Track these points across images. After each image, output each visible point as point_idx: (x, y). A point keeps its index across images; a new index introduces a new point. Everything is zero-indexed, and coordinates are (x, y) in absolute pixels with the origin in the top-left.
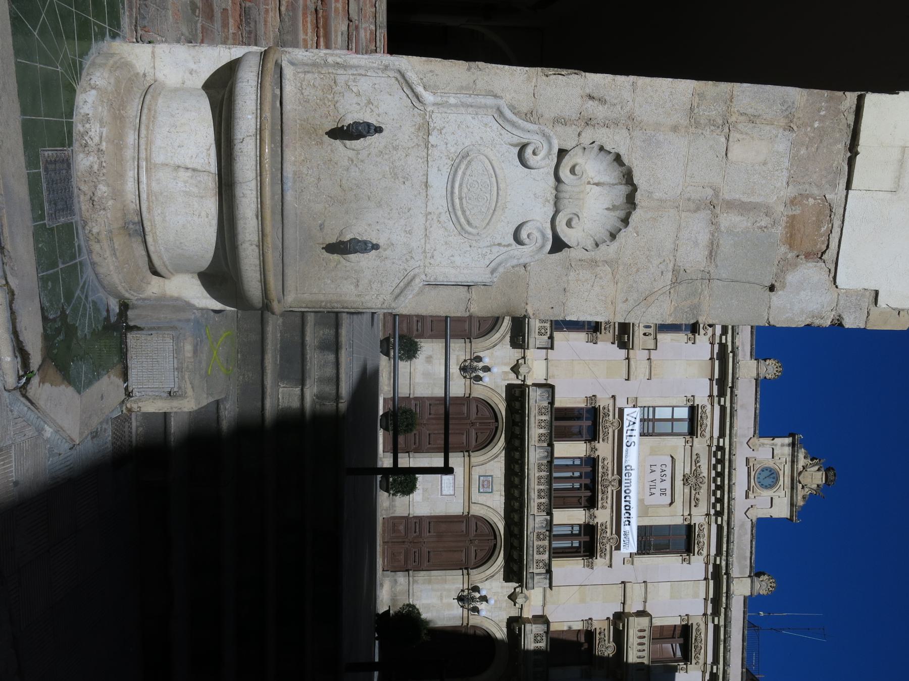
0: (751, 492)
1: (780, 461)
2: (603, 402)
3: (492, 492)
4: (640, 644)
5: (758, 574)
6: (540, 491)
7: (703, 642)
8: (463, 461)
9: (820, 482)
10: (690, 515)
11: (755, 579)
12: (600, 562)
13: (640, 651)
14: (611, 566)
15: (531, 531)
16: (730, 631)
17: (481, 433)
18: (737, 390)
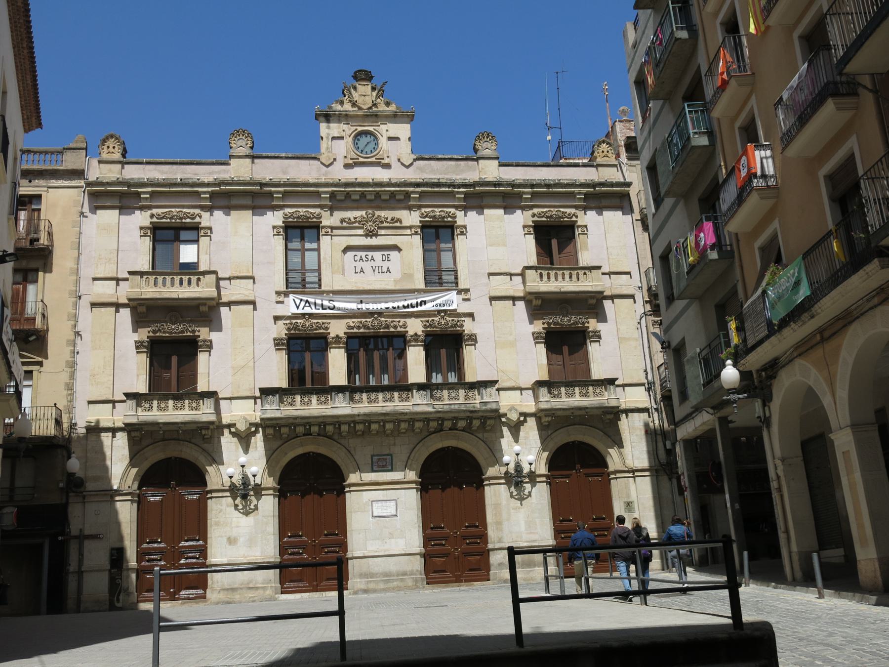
0: (383, 161)
1: (346, 130)
2: (280, 330)
3: (391, 455)
4: (556, 279)
5: (476, 151)
6: (385, 401)
7: (552, 209)
9: (370, 87)
10: (410, 227)
11: (479, 154)
12: (469, 327)
13: (563, 278)
14: (471, 315)
15: (431, 408)
16: (538, 180)
18: (265, 178)
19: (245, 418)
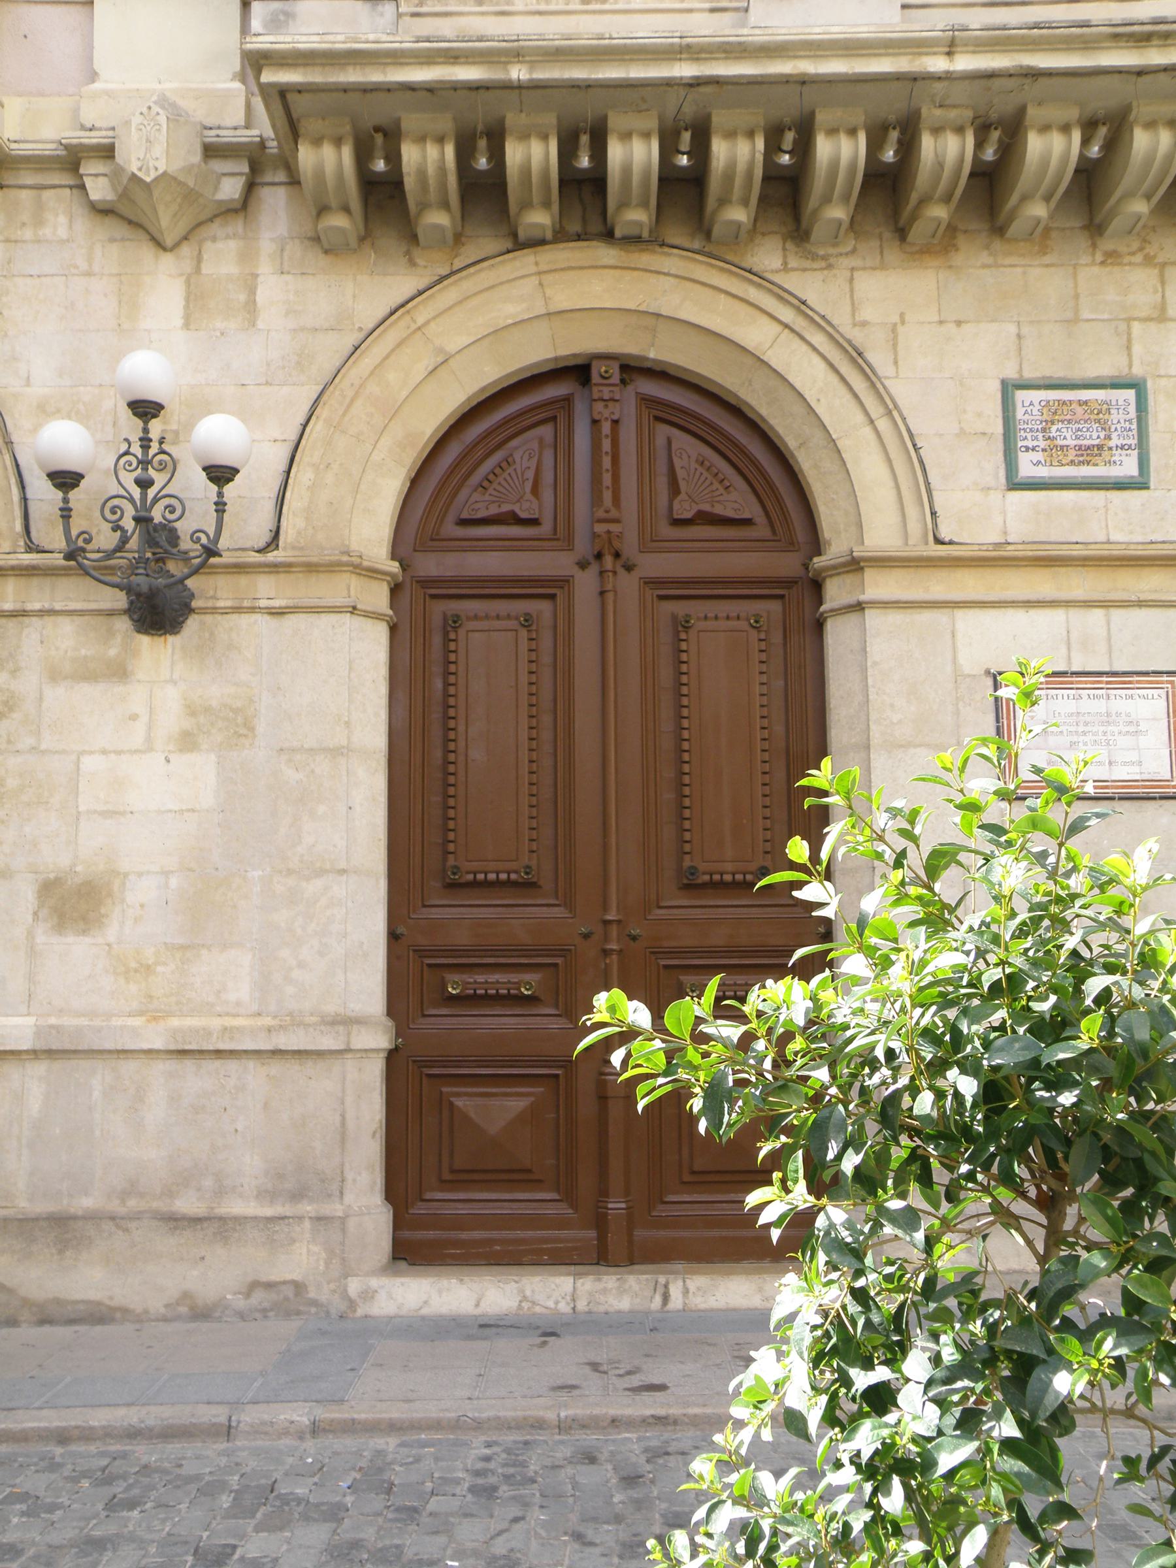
3: (1137, 386)
8: (895, 618)
17: (674, 489)
19: (176, 116)
